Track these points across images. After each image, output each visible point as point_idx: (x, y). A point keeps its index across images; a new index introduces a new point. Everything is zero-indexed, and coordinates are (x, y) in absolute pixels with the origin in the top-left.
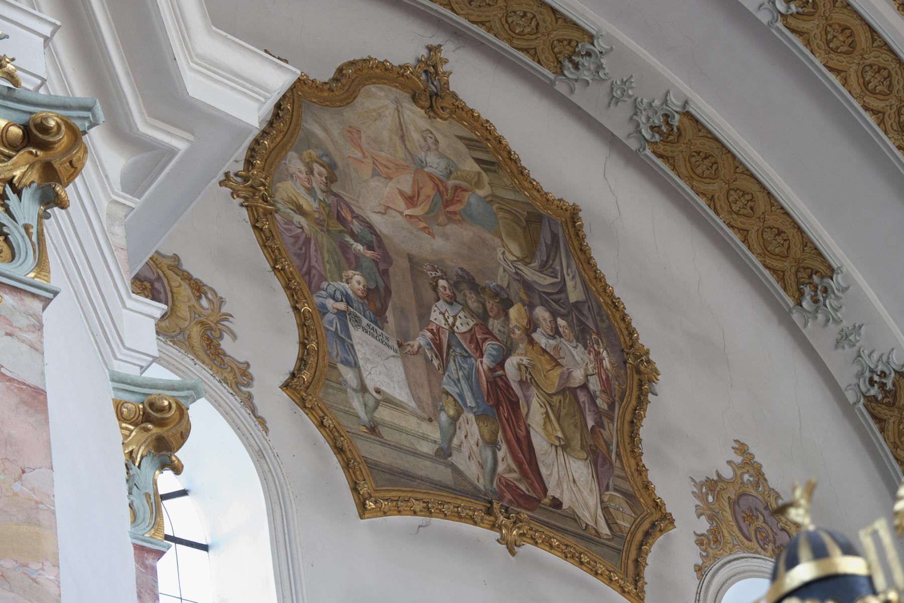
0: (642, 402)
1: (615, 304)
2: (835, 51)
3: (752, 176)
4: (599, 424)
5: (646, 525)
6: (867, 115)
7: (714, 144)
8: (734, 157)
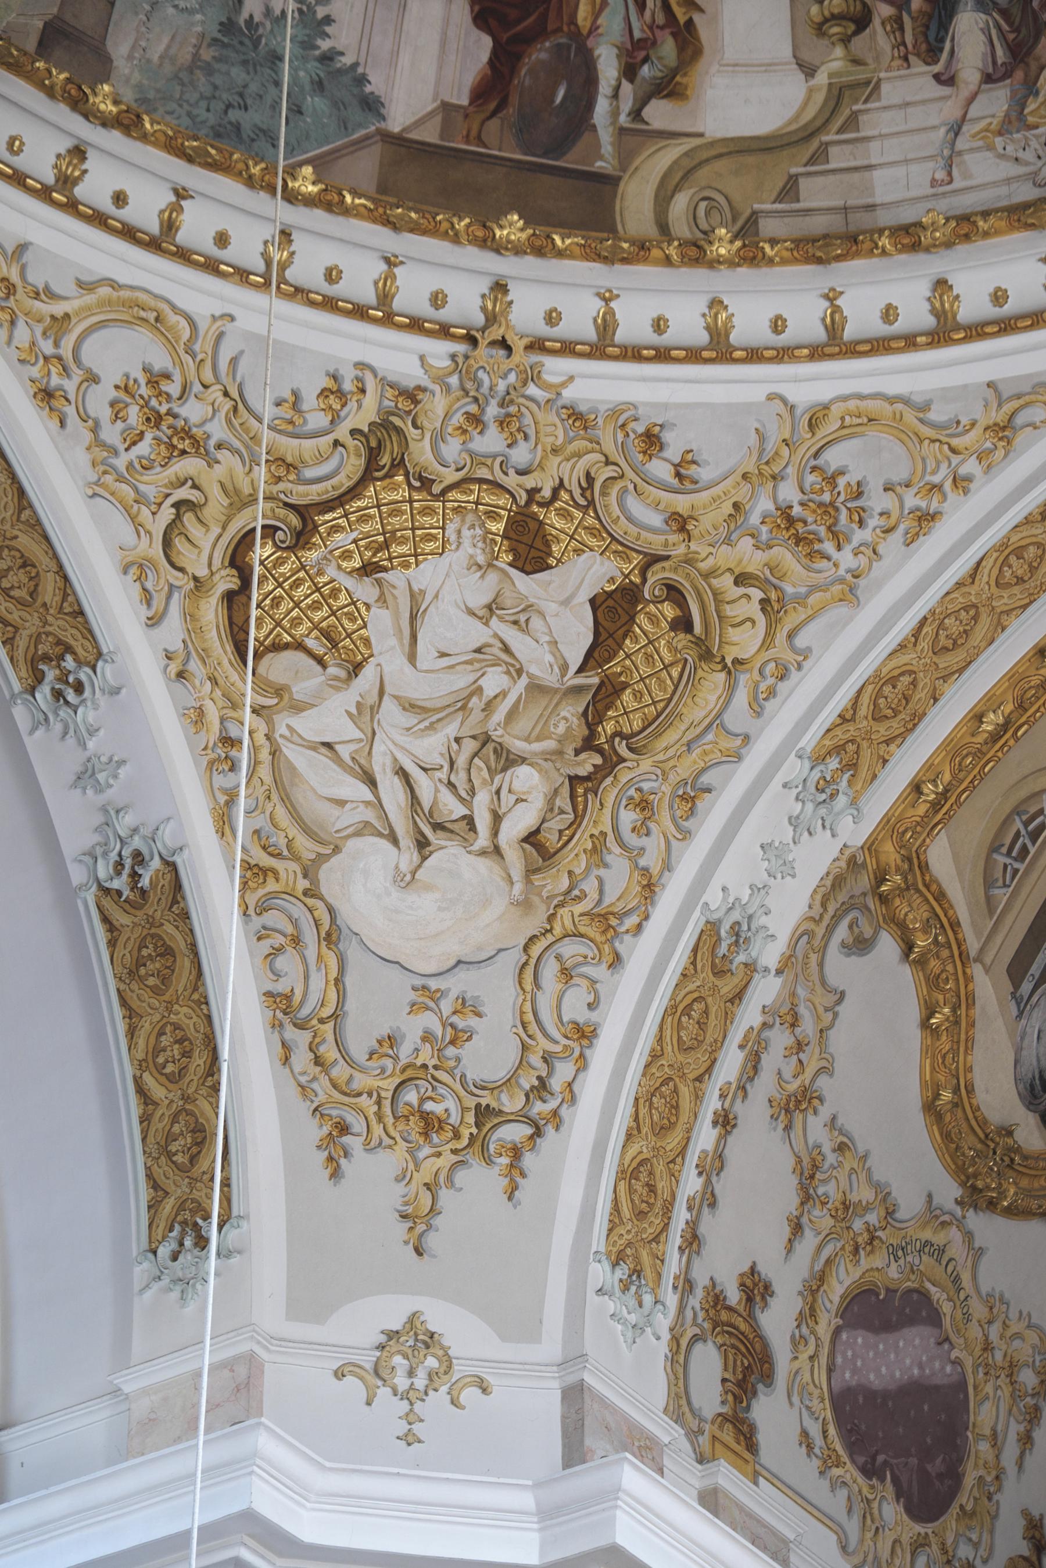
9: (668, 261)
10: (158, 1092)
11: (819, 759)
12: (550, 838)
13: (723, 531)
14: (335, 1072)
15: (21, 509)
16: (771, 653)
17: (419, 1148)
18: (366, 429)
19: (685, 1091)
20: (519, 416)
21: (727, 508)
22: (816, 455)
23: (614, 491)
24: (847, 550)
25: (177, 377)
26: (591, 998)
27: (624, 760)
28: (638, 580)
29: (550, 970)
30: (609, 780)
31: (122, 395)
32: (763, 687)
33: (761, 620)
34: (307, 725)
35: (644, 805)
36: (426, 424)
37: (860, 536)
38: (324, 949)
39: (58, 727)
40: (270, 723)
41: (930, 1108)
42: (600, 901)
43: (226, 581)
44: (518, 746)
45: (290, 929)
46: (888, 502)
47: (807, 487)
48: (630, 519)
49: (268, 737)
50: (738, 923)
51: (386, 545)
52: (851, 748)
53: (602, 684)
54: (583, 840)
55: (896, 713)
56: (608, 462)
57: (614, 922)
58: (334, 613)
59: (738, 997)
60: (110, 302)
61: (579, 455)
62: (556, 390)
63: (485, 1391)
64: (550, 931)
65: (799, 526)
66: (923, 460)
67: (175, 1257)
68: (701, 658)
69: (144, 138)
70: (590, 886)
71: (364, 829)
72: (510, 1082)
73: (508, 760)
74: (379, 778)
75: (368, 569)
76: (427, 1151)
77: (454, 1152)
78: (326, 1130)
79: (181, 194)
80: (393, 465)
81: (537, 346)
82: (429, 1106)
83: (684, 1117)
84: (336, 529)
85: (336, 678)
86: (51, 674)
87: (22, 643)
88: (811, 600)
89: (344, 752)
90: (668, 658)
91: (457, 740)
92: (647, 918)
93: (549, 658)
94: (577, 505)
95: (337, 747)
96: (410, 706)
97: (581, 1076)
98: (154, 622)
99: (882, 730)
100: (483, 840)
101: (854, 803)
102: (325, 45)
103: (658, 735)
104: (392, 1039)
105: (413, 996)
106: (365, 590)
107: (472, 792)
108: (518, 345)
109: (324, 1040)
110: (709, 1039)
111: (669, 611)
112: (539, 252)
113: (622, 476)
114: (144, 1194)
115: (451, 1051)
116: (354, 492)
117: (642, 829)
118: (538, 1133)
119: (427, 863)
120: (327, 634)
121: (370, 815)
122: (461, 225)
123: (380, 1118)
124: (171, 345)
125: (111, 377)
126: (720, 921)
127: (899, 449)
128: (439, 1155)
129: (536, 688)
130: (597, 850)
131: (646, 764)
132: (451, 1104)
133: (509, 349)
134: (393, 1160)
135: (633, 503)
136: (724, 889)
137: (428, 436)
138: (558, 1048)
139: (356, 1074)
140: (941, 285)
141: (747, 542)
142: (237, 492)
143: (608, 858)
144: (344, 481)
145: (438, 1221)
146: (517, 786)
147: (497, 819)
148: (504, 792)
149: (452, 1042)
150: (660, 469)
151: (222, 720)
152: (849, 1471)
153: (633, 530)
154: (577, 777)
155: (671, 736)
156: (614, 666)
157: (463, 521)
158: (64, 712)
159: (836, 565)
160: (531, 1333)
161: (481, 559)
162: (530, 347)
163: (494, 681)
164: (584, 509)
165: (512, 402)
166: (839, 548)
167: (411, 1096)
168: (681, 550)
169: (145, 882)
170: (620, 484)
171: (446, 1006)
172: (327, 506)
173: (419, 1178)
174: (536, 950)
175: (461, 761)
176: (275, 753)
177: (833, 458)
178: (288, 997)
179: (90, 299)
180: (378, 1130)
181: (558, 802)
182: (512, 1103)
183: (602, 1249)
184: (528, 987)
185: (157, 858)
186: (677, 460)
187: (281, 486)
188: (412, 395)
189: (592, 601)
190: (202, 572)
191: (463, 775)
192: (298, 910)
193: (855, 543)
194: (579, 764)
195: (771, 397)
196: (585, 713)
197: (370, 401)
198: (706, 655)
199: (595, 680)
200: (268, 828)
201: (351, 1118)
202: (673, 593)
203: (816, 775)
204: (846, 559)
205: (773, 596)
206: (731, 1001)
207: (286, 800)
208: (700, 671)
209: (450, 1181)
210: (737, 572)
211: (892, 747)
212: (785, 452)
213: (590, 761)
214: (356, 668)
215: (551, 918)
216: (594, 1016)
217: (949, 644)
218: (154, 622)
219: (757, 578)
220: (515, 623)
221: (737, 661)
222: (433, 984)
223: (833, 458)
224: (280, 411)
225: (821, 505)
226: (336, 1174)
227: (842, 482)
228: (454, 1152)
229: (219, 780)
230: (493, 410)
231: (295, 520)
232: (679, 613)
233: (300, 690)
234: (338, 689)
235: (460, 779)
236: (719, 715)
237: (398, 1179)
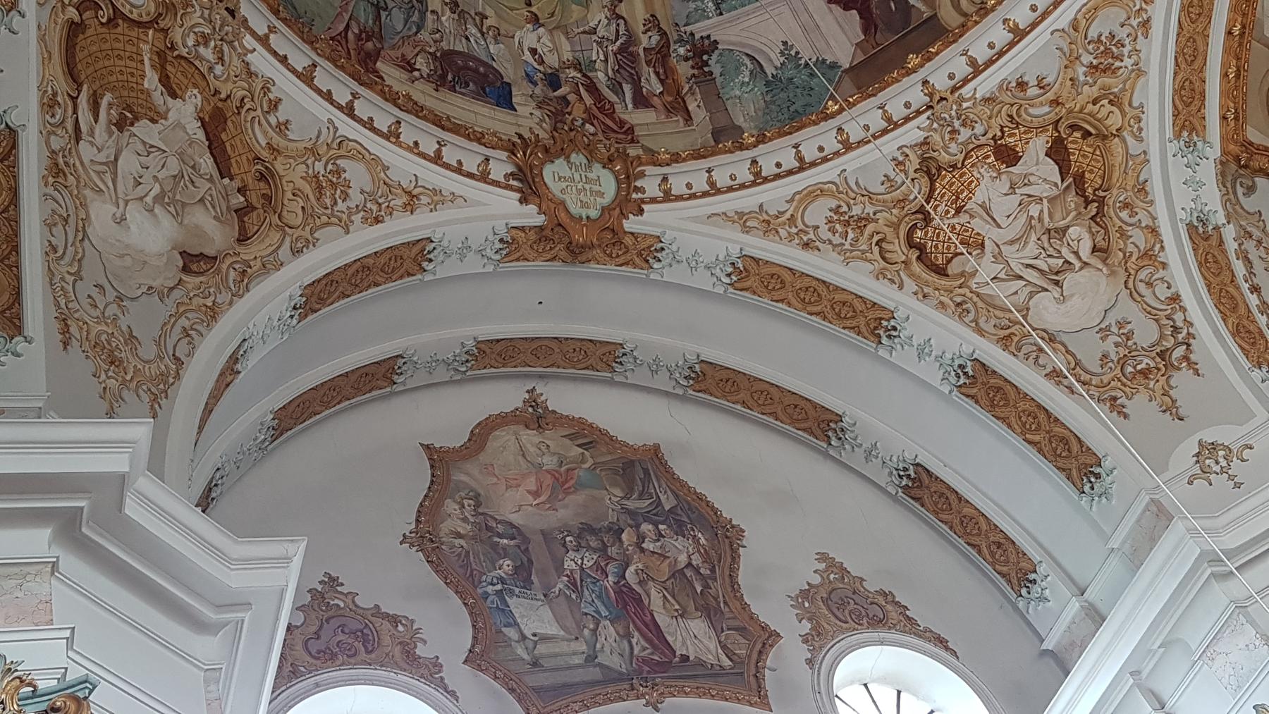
0: (735, 557)
1: (700, 497)
2: (774, 289)
3: (761, 380)
4: (706, 586)
5: (759, 646)
6: (813, 318)
7: (728, 371)
8: (745, 374)
9: (977, 23)
10: (1037, 438)
11: (1178, 136)
12: (1103, 244)
13: (1073, 91)
14: (1094, 383)
15: (828, 288)
16: (1128, 117)
17: (1148, 384)
18: (919, 167)
19: (1231, 289)
20: (967, 117)
21: (1069, 83)
22: (1086, 39)
23: (1023, 113)
24: (1126, 59)
25: (843, 204)
26: (1166, 285)
27: (1105, 197)
28: (1057, 134)
29: (1142, 287)
30: (1106, 208)
31: (830, 225)
32: (1135, 130)
33: (1114, 109)
35: (1126, 205)
36: (938, 148)
37: (1126, 51)
38: (1053, 345)
39: (899, 346)
40: (969, 287)
42: (1139, 251)
43: (914, 255)
45: (1035, 348)
46: (1127, 30)
47: (1093, 51)
48: (1036, 117)
49: (971, 292)
50: (1198, 217)
51: (958, 198)
52: (1187, 123)
53: (1074, 179)
54: (1114, 235)
55: (1194, 98)
56: (1012, 105)
57: (1151, 253)
58: (959, 234)
59: (1221, 242)
60: (801, 201)
61: (1000, 112)
62: (973, 97)
63: (1251, 448)
64: (1130, 274)
65: (1101, 66)
66: (1127, 5)
67: (1092, 488)
68: (1103, 140)
69: (771, 140)
70: (1131, 248)
71: (1031, 295)
72: (1162, 336)
74: (1021, 274)
75: (958, 211)
76: (1152, 383)
77: (1163, 375)
78: (1108, 404)
79: (796, 146)
80: (938, 171)
81: (954, 89)
82: (1139, 367)
83: (1239, 299)
84: (937, 206)
85: (978, 254)
86: (881, 332)
87: (864, 329)
88: (1127, 87)
89: (1002, 275)
90: (1091, 150)
91: (1039, 239)
92: (1162, 242)
93: (1047, 186)
94: (1013, 129)
95: (998, 276)
96: (1012, 242)
97: (1186, 313)
98: (901, 287)
99: (1193, 108)
100: (1078, 265)
101: (1205, 141)
102: (803, 62)
103: (1110, 178)
104: (1105, 356)
105: (1099, 335)
106: (964, 218)
107: (1059, 252)
108: (948, 95)
109: (1080, 375)
110: (1224, 265)
111: (1077, 134)
112: (929, 59)
113: (1021, 106)
114: (1063, 476)
115: (1130, 343)
116: (932, 190)
118: (1188, 345)
119: (1064, 288)
121: (1029, 289)
122: (895, 75)
123: (1125, 385)
124: (832, 196)
125: (821, 222)
126: (1191, 221)
127: (1116, 9)
128: (1158, 381)
129: (1051, 200)
130: (1123, 234)
131: (1115, 191)
132: (1146, 360)
133: (945, 99)
134: (1142, 397)
135: (1031, 111)
136: (1183, 209)
137: (941, 151)
138: (1169, 311)
139: (1103, 377)
141: (1086, 87)
142: (893, 223)
143: (1129, 233)
144: (926, 189)
145: (1178, 404)
146: (1073, 237)
147: (1076, 253)
148: (1071, 243)
149: (1128, 340)
151: (951, 299)
153: (1041, 119)
154: (1093, 216)
155: (1116, 175)
156: (1073, 169)
157: (978, 168)
158: (896, 340)
159: (1126, 67)
161: (995, 175)
162: (952, 92)
163: (1034, 210)
164: (1017, 127)
165: (961, 115)
166: (1122, 61)
167: (1130, 369)
168: (1064, 110)
169: (971, 373)
170: (1023, 108)
171: (1115, 330)
174: (1130, 285)
175: (1046, 245)
176: (978, 295)
177: (1092, 34)
178: (1054, 370)
179: (795, 203)
180: (1127, 390)
181: (1093, 230)
182: (1169, 343)
183: (1250, 366)
184: (1139, 300)
185: (968, 362)
186: (1036, 83)
187: (906, 209)
188: (925, 142)
189: (1046, 155)
190: (904, 258)
191: (1051, 249)
193: (1127, 54)
194: (1089, 212)
195: (1052, 34)
196: (1077, 193)
197: (912, 156)
198: (1105, 137)
199: (1071, 179)
200: (998, 321)
201: (1113, 394)
202: (1074, 127)
203: (1182, 143)
204: (1128, 62)
205: (1112, 97)
206: (1220, 245)
207: (995, 307)
208: (1107, 145)
209: (1171, 388)
210: (1091, 100)
211: (1202, 111)
212: (1073, 46)
213: (1093, 208)
214: (983, 245)
215: (1126, 270)
216: (1173, 290)
217: (1192, 58)
218: (901, 287)
219: (1100, 96)
220: (1025, 185)
221: (1117, 130)
222: (1103, 326)
223: (1092, 34)
224: (885, 186)
225: (1102, 53)
226: (1126, 416)
227: (1103, 38)
228: (1163, 375)
229: (967, 320)
230: (957, 124)
231: (920, 216)
232: (1081, 132)
234: (982, 257)
235: (1051, 251)
236: (1127, 153)
237: (1150, 401)
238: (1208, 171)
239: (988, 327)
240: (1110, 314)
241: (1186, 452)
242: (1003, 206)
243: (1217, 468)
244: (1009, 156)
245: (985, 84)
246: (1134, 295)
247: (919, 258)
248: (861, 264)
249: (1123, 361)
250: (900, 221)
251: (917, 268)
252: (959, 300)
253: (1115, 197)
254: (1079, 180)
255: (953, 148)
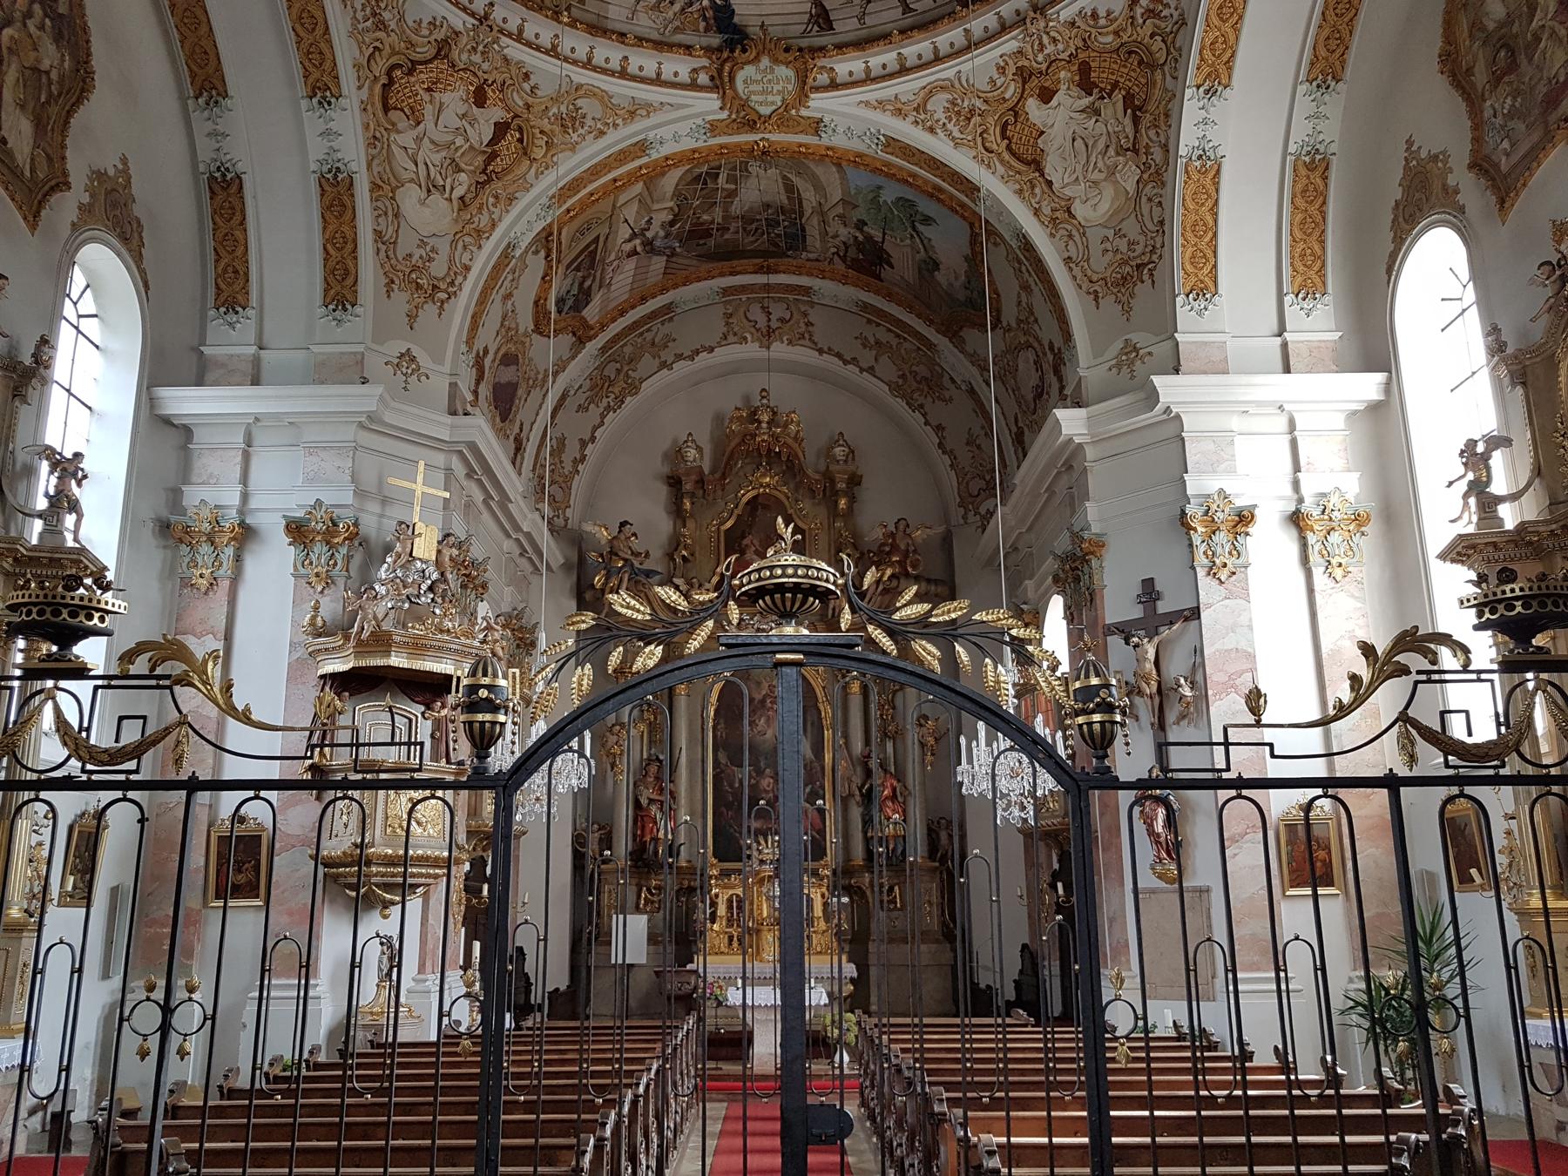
0: (79, 101)
4: (48, 102)
10: (332, 252)
12: (467, 200)
29: (460, 244)
34: (401, 139)
35: (496, 197)
41: (536, 303)
43: (384, 80)
44: (463, 166)
46: (591, 123)
51: (435, 83)
54: (477, 203)
62: (503, 48)
67: (334, 310)
71: (412, 181)
73: (460, 170)
75: (429, 90)
89: (410, 151)
96: (432, 142)
98: (359, 88)
100: (447, 195)
104: (410, 255)
106: (426, 97)
108: (495, 29)
114: (324, 286)
116: (430, 61)
117: (494, 205)
120: (411, 108)
121: (414, 176)
129: (472, 147)
130: (480, 208)
131: (500, 184)
134: (405, 296)
140: (626, 58)
144: (428, 56)
147: (452, 189)
150: (526, 86)
152: (492, 407)
155: (510, 177)
160: (442, 363)
163: (459, 141)
167: (414, 276)
171: (428, 248)
172: (421, 63)
173: (415, 304)
177: (579, 103)
182: (443, 286)
188: (457, 33)
192: (388, 203)
202: (520, 130)
207: (389, 163)
214: (419, 123)
218: (359, 88)
226: (389, 296)
230: (481, 48)
233: (400, 126)
235: (443, 172)
238: (541, 225)
239: (376, 170)
240: (434, 239)
241: (396, 347)
242: (450, 118)
243: (404, 370)
244: (480, 99)
245: (515, 51)
246: (454, 243)
247: (384, 85)
248: (356, 46)
249: (415, 268)
250: (398, 53)
251: (378, 89)
252: (378, 135)
253: (497, 186)
254: (493, 156)
255: (464, 57)
